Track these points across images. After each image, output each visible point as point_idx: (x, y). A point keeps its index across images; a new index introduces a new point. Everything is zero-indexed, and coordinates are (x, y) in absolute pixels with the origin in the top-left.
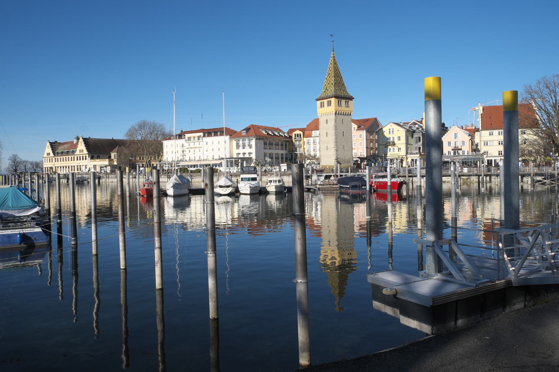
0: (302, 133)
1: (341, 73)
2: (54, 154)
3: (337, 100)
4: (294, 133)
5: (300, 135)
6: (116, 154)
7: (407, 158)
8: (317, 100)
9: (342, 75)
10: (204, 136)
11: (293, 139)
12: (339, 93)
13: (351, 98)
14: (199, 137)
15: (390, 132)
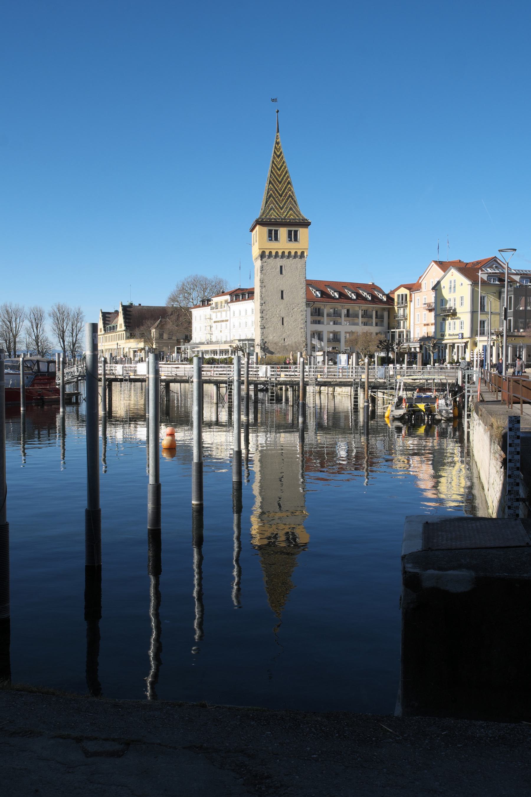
0: (407, 292)
1: (291, 173)
2: (105, 330)
3: (265, 230)
4: (397, 293)
5: (406, 295)
6: (154, 330)
7: (475, 344)
8: (252, 230)
9: (292, 179)
10: (232, 301)
11: (396, 304)
12: (273, 215)
13: (306, 224)
14: (226, 302)
15: (450, 288)
